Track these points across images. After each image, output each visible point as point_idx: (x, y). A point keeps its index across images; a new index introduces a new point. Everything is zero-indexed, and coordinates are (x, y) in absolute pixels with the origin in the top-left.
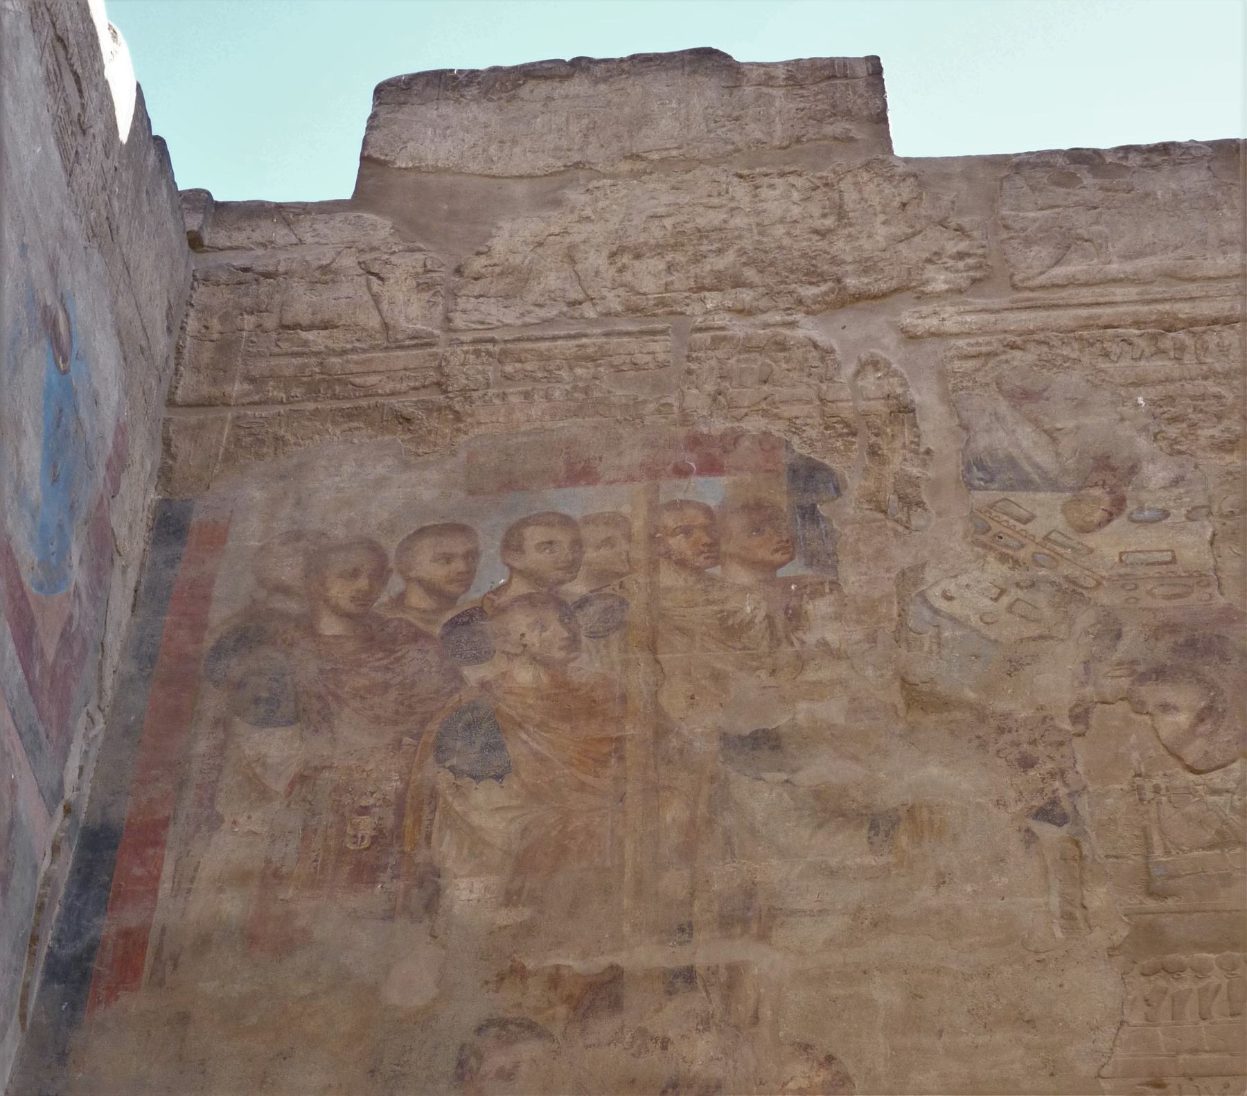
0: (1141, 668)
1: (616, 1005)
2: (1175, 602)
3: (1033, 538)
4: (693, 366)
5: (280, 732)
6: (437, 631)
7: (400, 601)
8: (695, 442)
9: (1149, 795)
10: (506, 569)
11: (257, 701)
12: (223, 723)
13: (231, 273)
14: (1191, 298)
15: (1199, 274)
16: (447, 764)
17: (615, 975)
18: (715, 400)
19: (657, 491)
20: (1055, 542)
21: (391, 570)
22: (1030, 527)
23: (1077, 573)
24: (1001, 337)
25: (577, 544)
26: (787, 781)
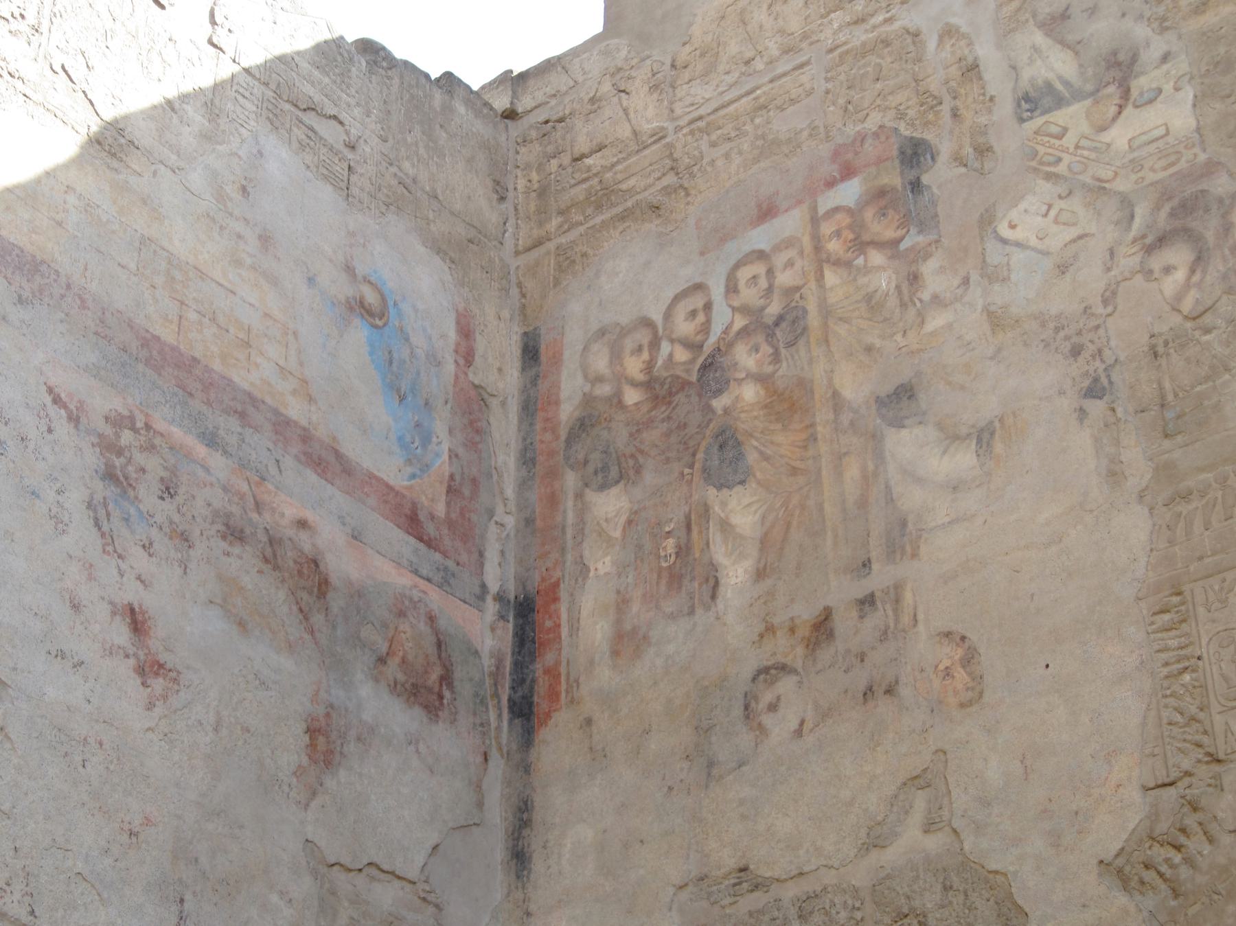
0: (1148, 241)
1: (831, 635)
3: (1066, 151)
4: (830, 86)
5: (614, 491)
9: (1161, 349)
10: (730, 310)
13: (538, 129)
18: (846, 110)
20: (1083, 148)
25: (770, 272)
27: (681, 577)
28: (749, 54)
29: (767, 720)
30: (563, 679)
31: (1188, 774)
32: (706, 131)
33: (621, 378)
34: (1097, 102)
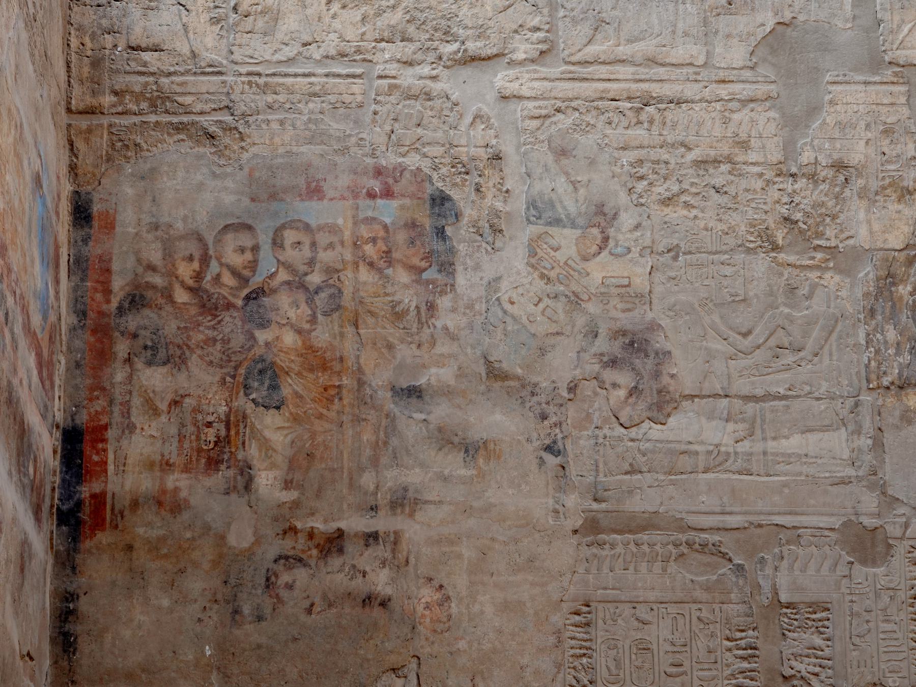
0: (605, 359)
1: (341, 551)
2: (627, 315)
5: (164, 370)
6: (240, 303)
7: (217, 278)
8: (379, 172)
10: (275, 261)
11: (146, 347)
12: (128, 360)
15: (667, 61)
16: (251, 397)
17: (340, 533)
19: (357, 208)
20: (570, 267)
21: (211, 257)
22: (557, 254)
23: (579, 290)
24: (553, 102)
25: (314, 244)
26: (425, 420)
27: (218, 462)
28: (307, 38)
29: (284, 594)
30: (108, 507)
32: (265, 89)
33: (172, 274)
34: (584, 236)
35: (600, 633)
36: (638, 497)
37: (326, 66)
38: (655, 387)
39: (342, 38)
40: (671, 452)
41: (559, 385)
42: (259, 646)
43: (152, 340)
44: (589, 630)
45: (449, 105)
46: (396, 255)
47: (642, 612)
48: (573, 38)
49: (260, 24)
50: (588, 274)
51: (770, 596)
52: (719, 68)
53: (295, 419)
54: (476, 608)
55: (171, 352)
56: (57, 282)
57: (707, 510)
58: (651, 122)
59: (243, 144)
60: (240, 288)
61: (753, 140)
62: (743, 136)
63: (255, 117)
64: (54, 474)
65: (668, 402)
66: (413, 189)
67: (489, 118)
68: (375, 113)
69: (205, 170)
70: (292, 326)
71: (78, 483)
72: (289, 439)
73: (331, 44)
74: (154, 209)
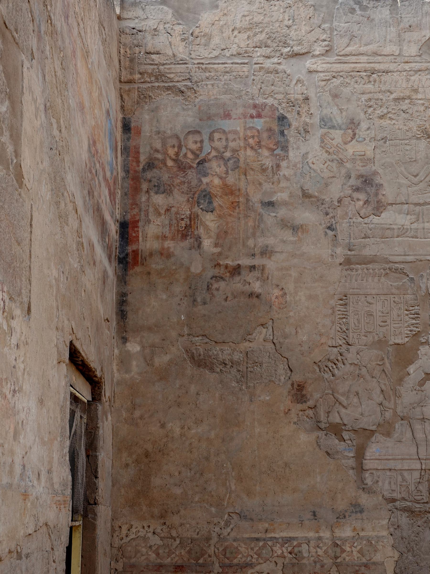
0: (354, 188)
1: (239, 274)
2: (364, 168)
5: (162, 196)
6: (195, 166)
7: (185, 155)
8: (255, 106)
11: (155, 186)
12: (147, 192)
14: (379, 62)
15: (382, 53)
16: (201, 207)
17: (239, 266)
20: (339, 147)
25: (227, 139)
28: (224, 47)
29: (215, 292)
31: (341, 346)
32: (205, 70)
33: (166, 153)
34: (345, 134)
35: (351, 308)
36: (368, 249)
37: (232, 59)
38: (376, 200)
39: (239, 46)
40: (383, 229)
41: (333, 200)
42: (205, 315)
43: (157, 183)
44: (346, 307)
45: (286, 75)
46: (263, 143)
47: (369, 299)
48: (340, 44)
49: (203, 41)
50: (347, 150)
51: (425, 291)
52: (405, 56)
53: (219, 217)
54: (297, 298)
55: (166, 188)
56: (117, 158)
57: (398, 254)
58: (375, 81)
59: (196, 95)
60: (195, 159)
61: (420, 89)
62: (416, 87)
63: (201, 83)
64: (117, 242)
65: (381, 207)
66: (270, 113)
67: (303, 81)
68: (254, 80)
69: (180, 107)
70: (218, 175)
71: (127, 246)
72: (217, 225)
73: (234, 49)
74: (158, 125)
